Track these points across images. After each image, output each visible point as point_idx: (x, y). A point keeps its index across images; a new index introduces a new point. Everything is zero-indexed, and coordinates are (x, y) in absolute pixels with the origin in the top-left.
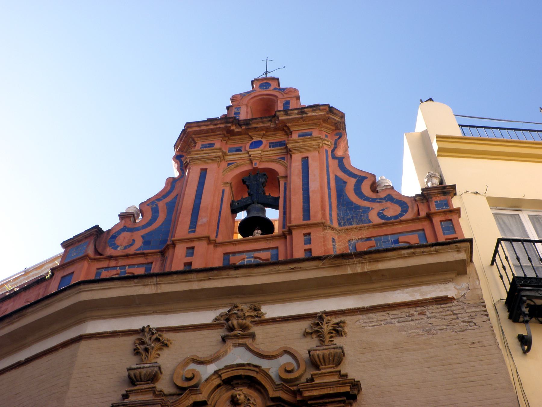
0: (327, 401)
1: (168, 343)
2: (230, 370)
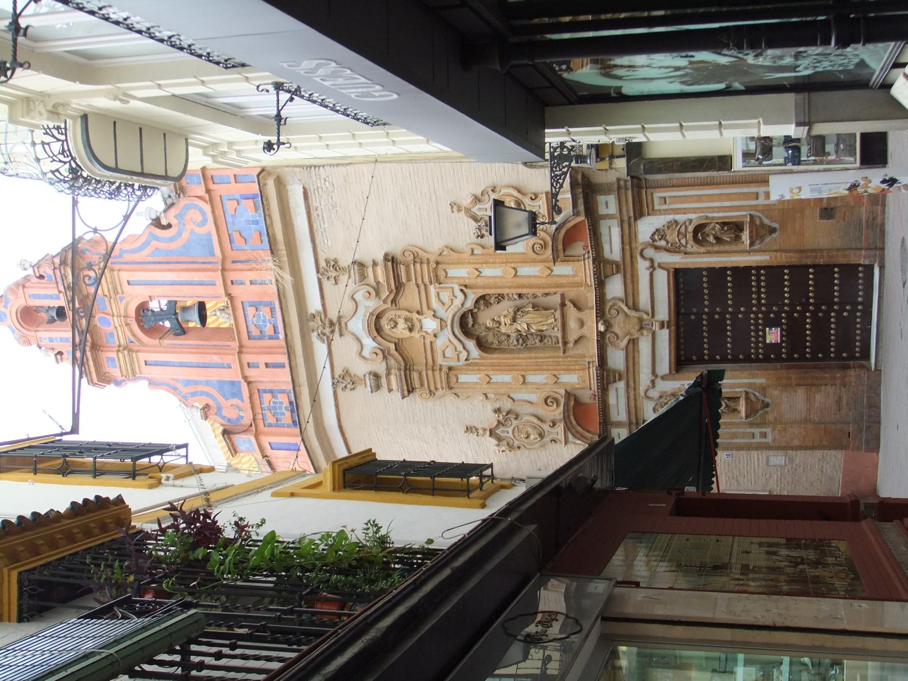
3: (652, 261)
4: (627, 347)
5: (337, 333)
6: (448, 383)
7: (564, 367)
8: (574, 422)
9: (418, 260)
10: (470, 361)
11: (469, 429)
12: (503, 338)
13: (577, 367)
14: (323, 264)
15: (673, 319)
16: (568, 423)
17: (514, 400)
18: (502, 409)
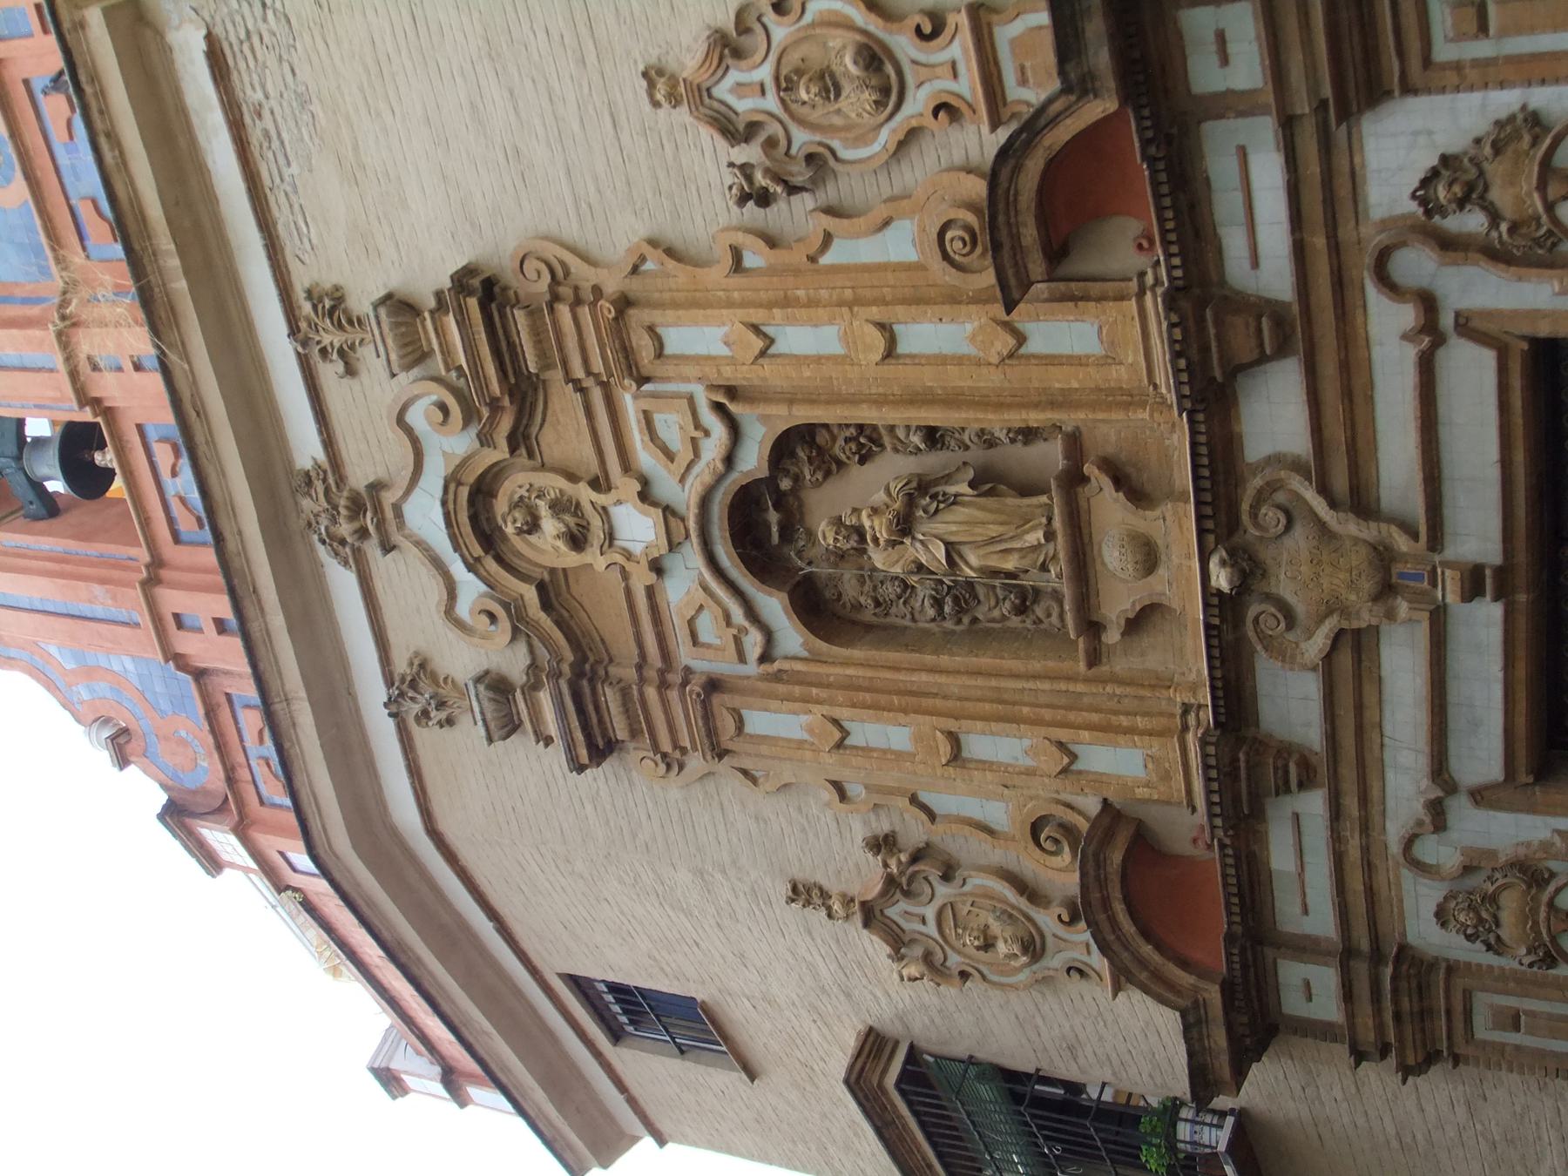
1: (416, 662)
2: (461, 541)
3: (1428, 303)
4: (1329, 658)
6: (711, 732)
7: (1095, 717)
10: (777, 665)
11: (800, 893)
12: (890, 590)
13: (1140, 722)
15: (1522, 558)
18: (902, 840)
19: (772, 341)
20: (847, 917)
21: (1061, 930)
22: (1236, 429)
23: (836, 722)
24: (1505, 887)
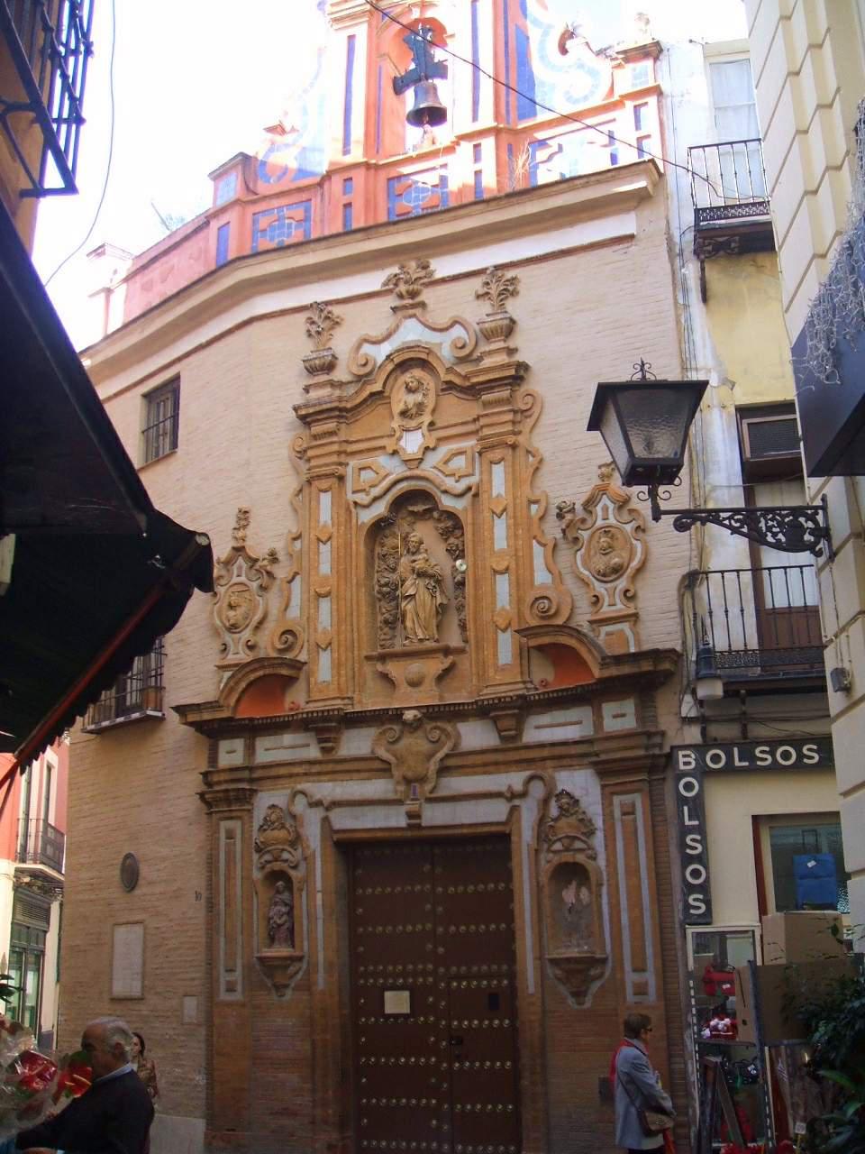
0: (493, 384)
1: (338, 320)
3: (524, 795)
4: (378, 758)
5: (398, 303)
6: (319, 477)
7: (343, 659)
8: (252, 677)
9: (519, 417)
10: (353, 510)
12: (391, 562)
13: (343, 679)
14: (510, 274)
15: (425, 833)
16: (251, 667)
17: (290, 582)
18: (276, 565)
19: (499, 517)
20: (236, 538)
21: (243, 641)
22: (471, 719)
23: (330, 538)
24: (289, 832)
